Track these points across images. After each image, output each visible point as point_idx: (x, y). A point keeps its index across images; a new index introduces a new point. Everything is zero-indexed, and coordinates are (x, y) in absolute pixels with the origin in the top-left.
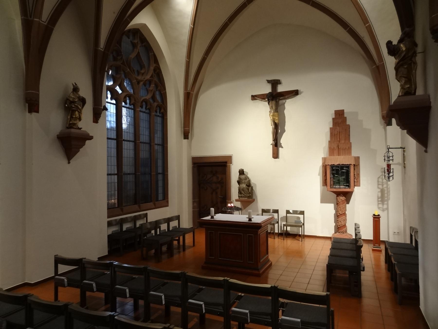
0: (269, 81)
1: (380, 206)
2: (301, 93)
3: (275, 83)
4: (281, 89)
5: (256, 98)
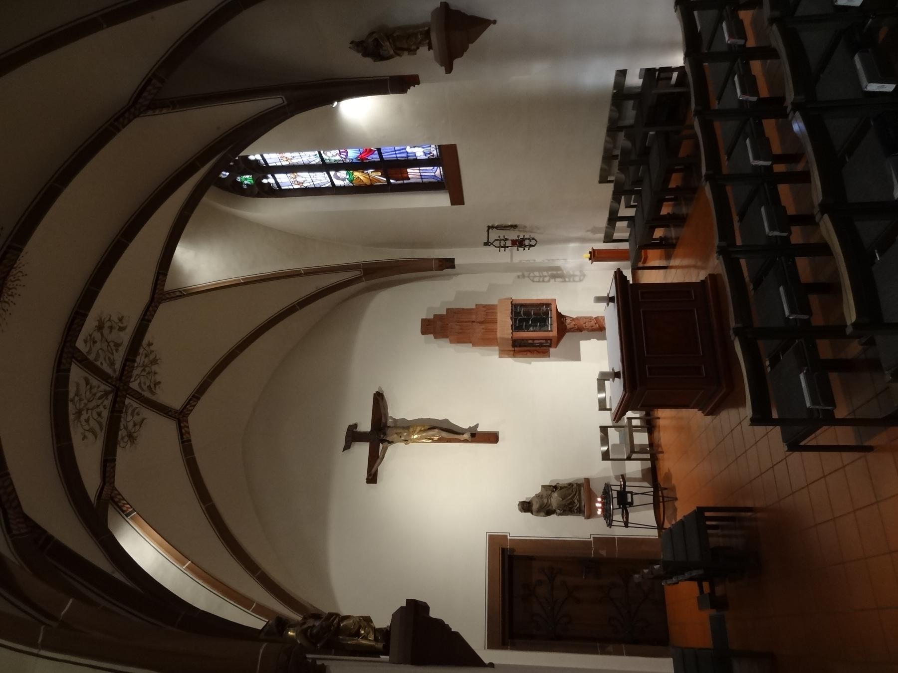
0: (347, 447)
1: (577, 279)
2: (380, 388)
3: (354, 436)
4: (366, 426)
5: (373, 470)
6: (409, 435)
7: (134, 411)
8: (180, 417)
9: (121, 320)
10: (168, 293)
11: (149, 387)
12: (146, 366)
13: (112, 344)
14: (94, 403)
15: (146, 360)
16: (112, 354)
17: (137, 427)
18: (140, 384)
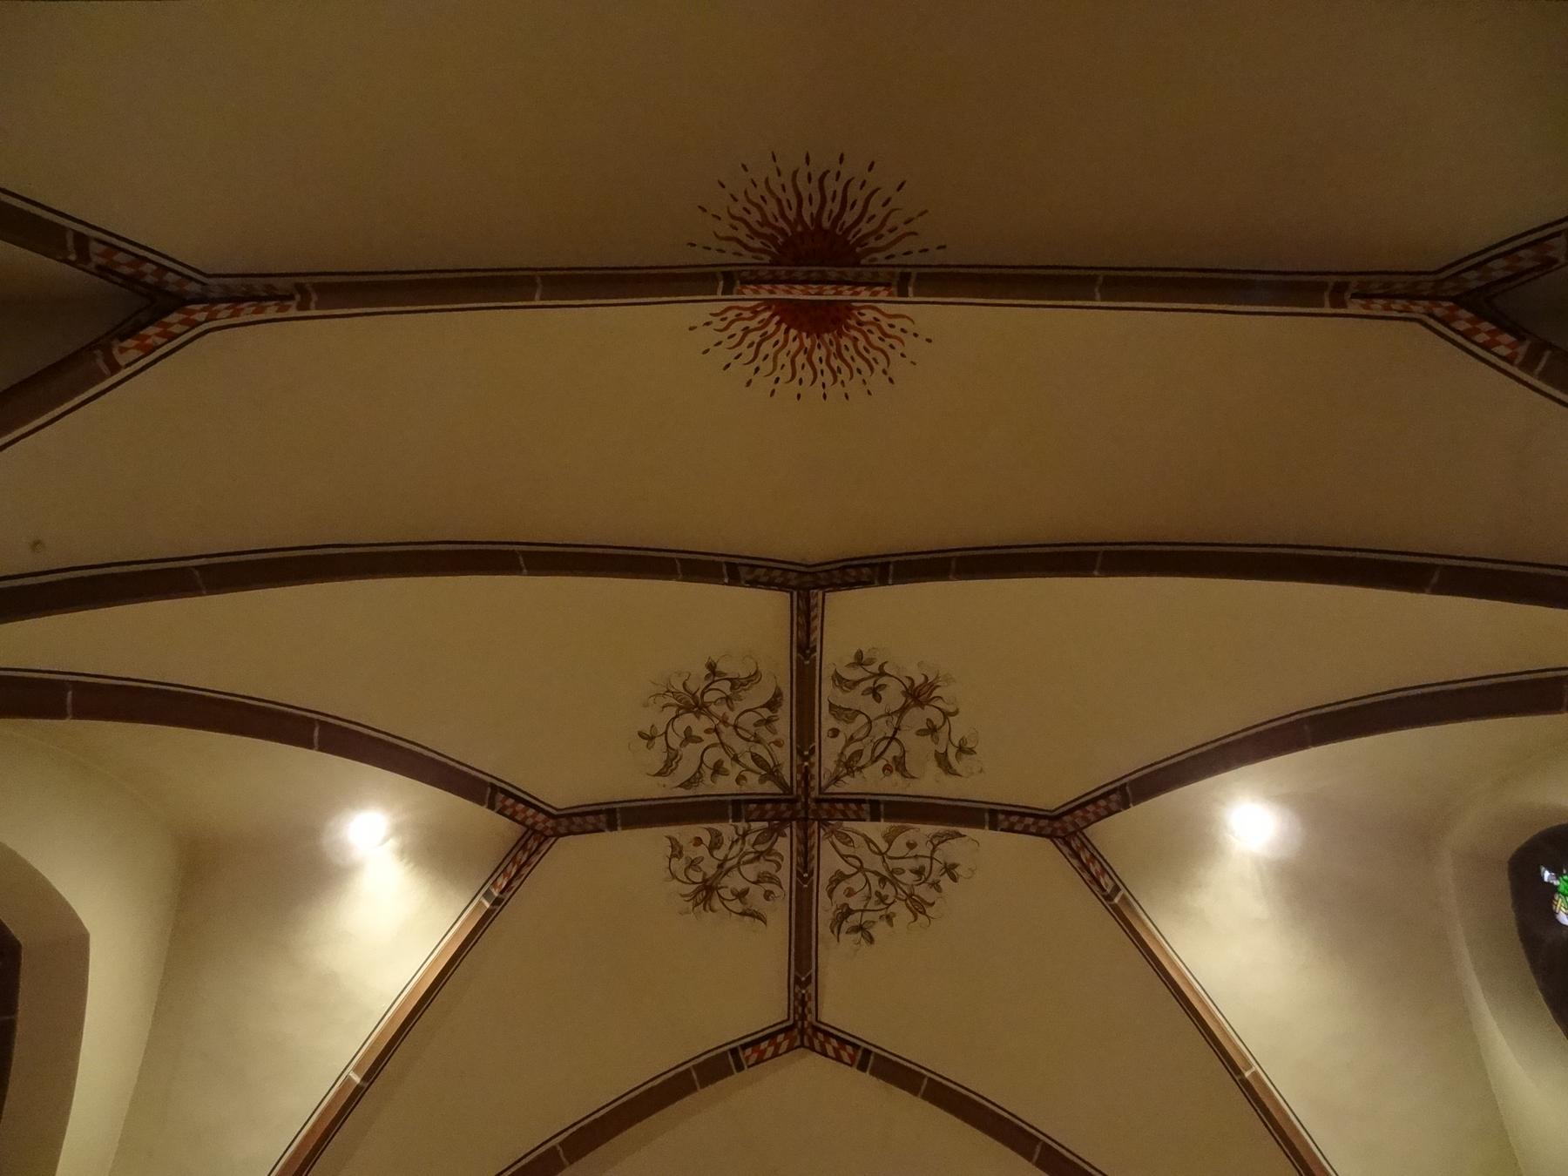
7: (772, 879)
8: (802, 1030)
9: (962, 750)
10: (1086, 844)
11: (850, 912)
12: (895, 883)
13: (894, 750)
14: (738, 745)
15: (908, 878)
16: (874, 760)
17: (737, 906)
18: (840, 877)
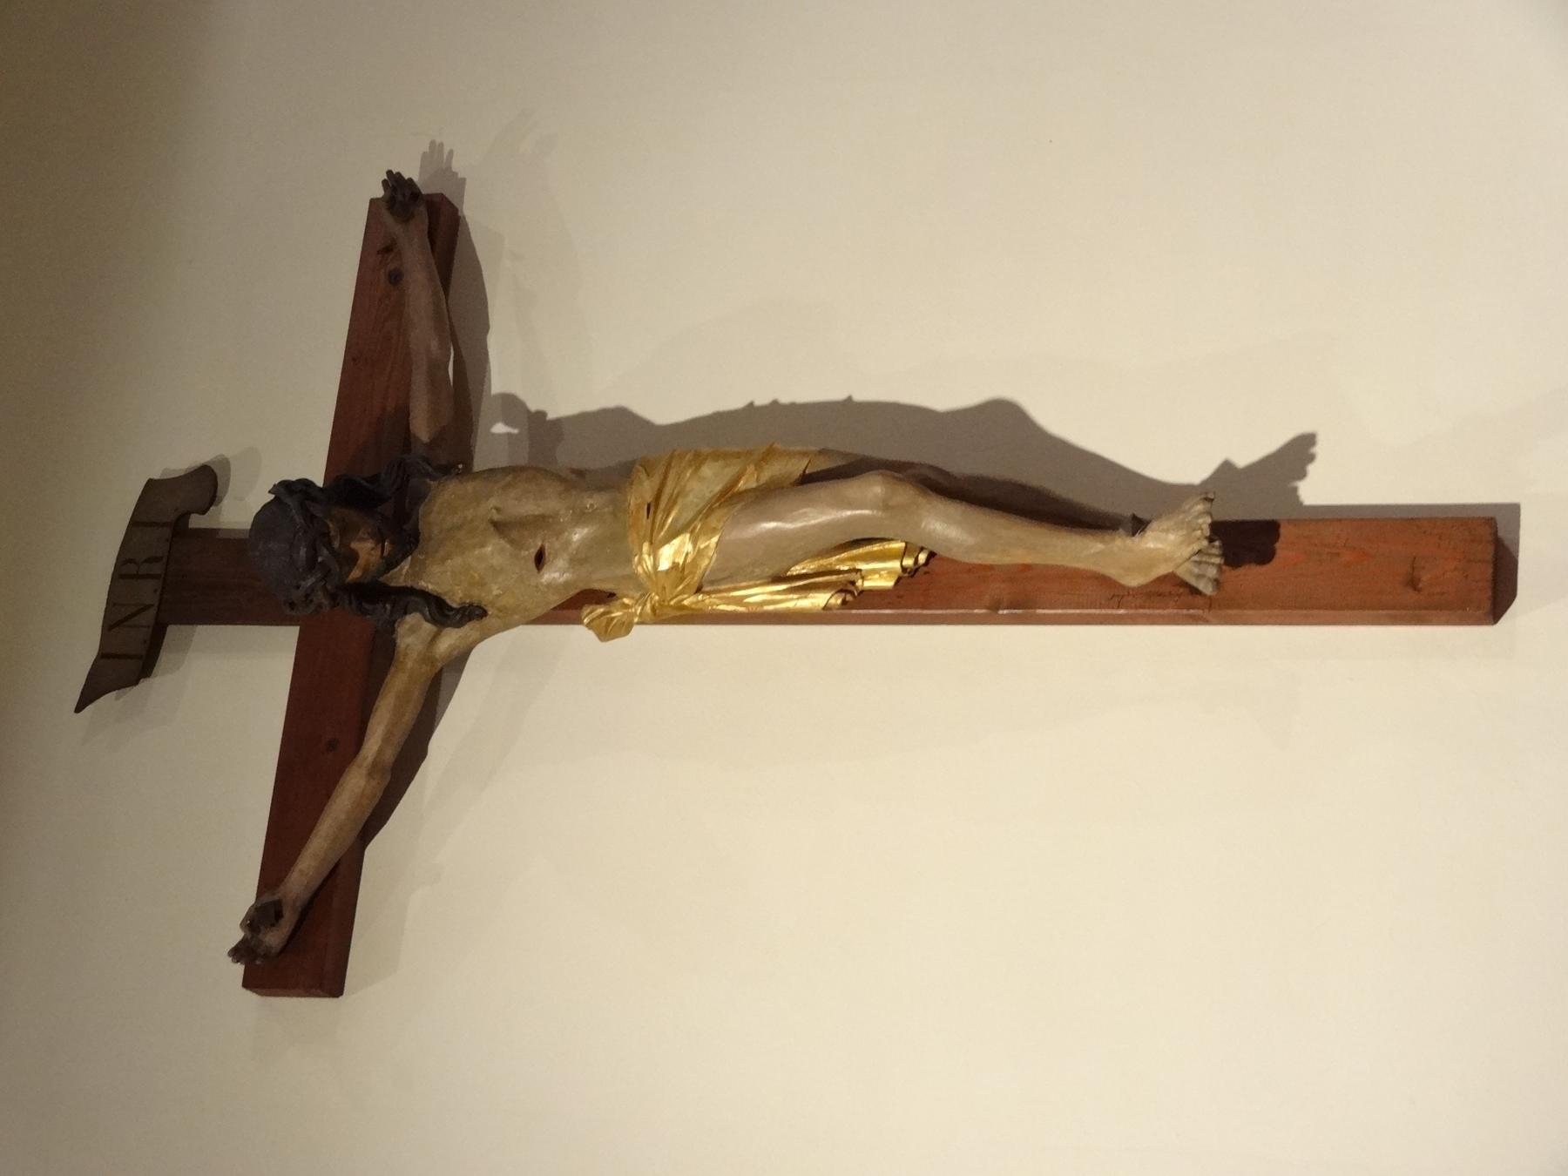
3: (178, 572)
6: (615, 548)
